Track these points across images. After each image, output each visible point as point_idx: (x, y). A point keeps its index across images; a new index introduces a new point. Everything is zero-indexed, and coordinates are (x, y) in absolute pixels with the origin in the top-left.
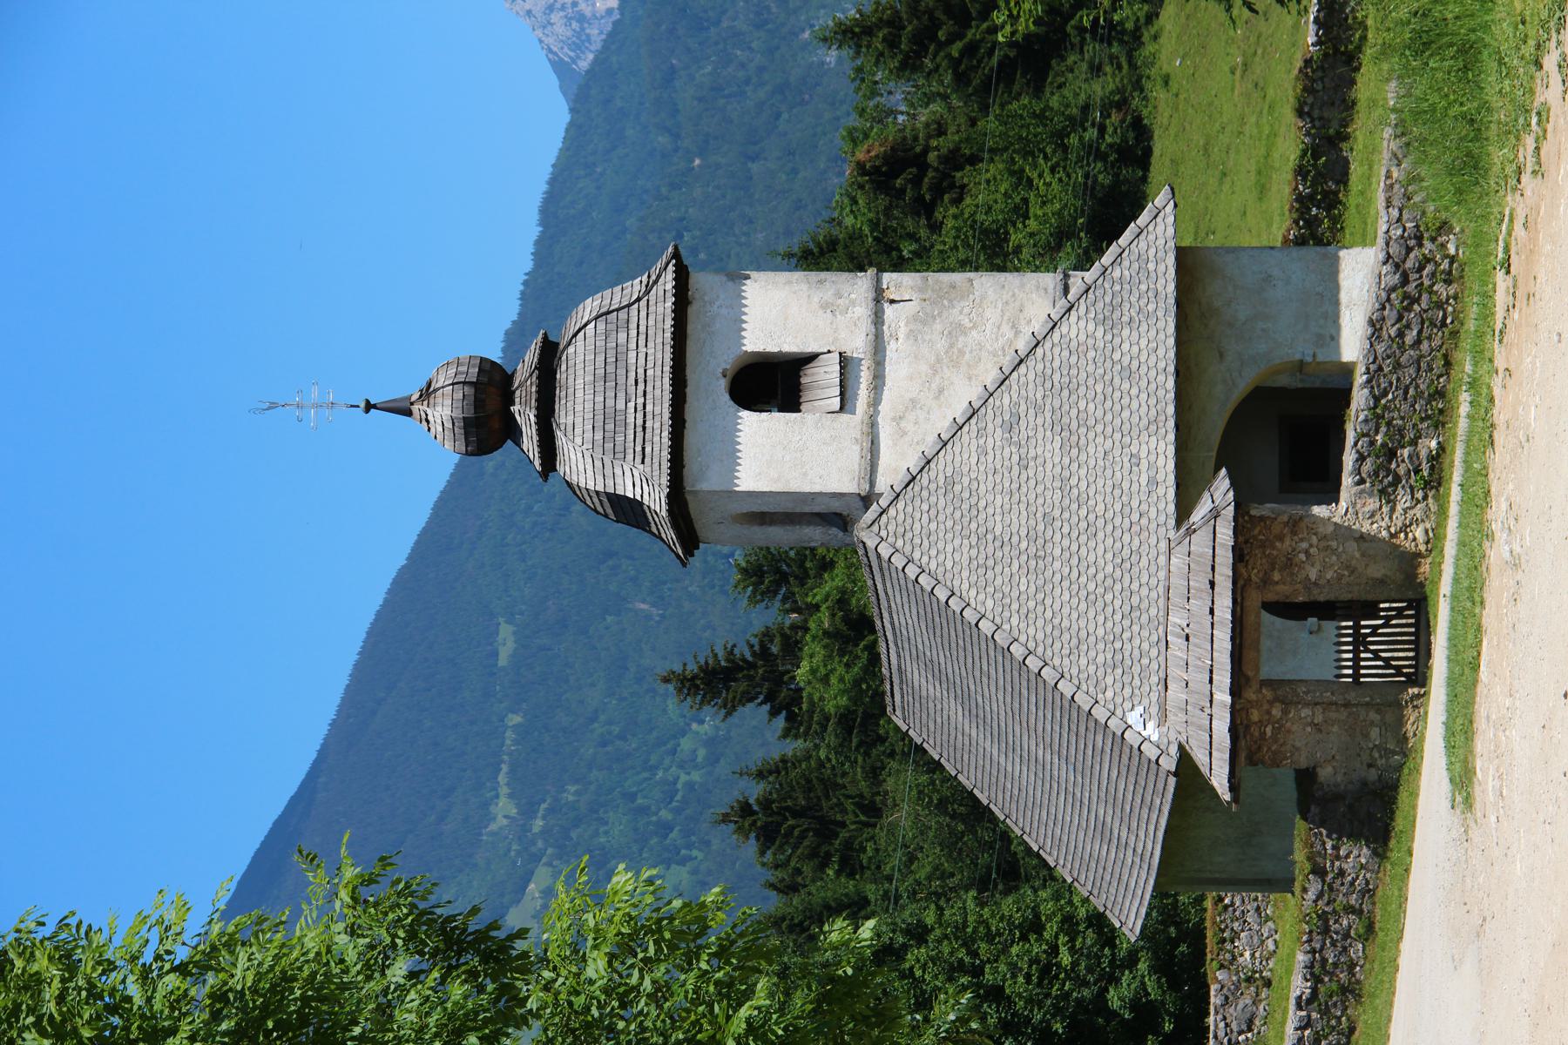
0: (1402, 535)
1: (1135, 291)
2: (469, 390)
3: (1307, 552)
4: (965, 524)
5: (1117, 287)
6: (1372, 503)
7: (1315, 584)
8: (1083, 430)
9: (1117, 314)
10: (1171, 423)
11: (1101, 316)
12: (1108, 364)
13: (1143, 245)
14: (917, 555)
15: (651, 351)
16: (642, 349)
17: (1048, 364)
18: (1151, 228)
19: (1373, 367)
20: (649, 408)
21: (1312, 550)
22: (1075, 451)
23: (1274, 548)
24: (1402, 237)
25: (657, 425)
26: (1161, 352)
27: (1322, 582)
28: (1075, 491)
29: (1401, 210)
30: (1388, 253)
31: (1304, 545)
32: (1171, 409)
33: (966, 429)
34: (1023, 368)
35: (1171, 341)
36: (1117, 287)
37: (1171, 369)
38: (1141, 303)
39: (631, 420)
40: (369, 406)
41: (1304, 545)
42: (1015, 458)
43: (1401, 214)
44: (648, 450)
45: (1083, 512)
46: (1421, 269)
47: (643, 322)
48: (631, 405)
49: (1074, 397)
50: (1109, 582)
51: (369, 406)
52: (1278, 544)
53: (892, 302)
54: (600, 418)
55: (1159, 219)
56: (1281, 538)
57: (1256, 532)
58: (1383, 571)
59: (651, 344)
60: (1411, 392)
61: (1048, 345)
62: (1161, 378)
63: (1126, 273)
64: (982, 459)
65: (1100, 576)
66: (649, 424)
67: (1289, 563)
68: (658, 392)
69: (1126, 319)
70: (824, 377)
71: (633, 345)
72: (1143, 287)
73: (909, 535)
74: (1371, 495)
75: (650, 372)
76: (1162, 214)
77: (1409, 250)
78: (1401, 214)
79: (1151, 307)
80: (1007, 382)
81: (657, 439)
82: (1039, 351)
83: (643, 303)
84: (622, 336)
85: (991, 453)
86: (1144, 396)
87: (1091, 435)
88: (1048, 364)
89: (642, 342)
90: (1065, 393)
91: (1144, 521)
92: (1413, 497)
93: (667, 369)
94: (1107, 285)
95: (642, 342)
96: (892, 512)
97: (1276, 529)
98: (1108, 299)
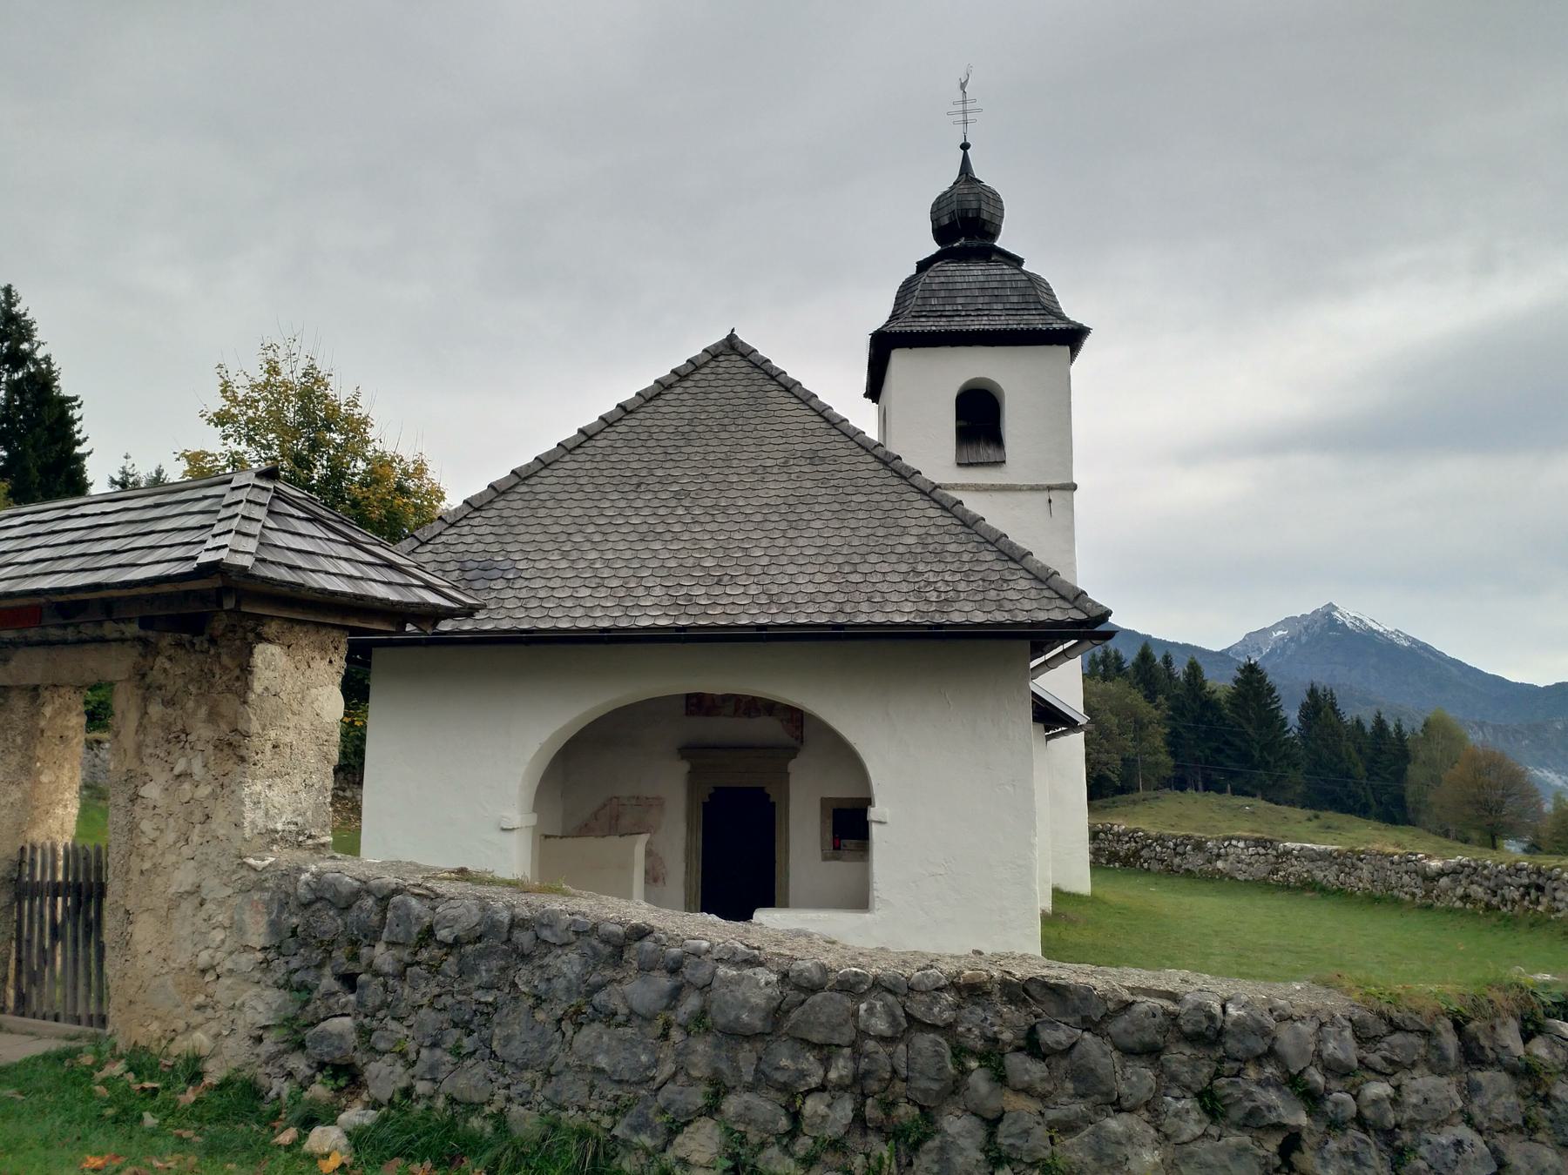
0: (200, 999)
1: (958, 577)
2: (974, 205)
3: (185, 775)
4: (705, 422)
5: (966, 557)
6: (258, 935)
7: (135, 798)
8: (783, 525)
9: (930, 558)
10: (763, 620)
11: (930, 540)
12: (864, 550)
13: (1024, 584)
14: (688, 384)
15: (1003, 318)
16: (1004, 312)
17: (877, 489)
18: (1047, 593)
19: (524, 939)
20: (957, 319)
21: (187, 786)
22: (759, 518)
23: (198, 705)
24: (864, 1034)
25: (941, 323)
26: (865, 607)
27: (138, 809)
28: (708, 518)
29: (947, 1029)
30: (814, 989)
31: (197, 768)
32: (781, 620)
33: (818, 419)
34: (876, 465)
35: (879, 618)
36: (966, 557)
37: (841, 619)
38: (939, 584)
39: (947, 308)
40: (965, 147)
41: (197, 768)
42: (769, 463)
43: (934, 1028)
44: (923, 319)
45: (677, 528)
46: (762, 1081)
47: (1026, 312)
48: (960, 308)
49: (828, 515)
50: (574, 555)
51: (965, 147)
52: (203, 712)
53: (1050, 501)
54: (950, 287)
55: (1059, 603)
56: (213, 717)
57: (226, 660)
58: (142, 949)
59: (1007, 318)
60: (468, 1044)
61: (904, 488)
62: (829, 607)
63: (985, 566)
64: (777, 434)
65: (587, 546)
66: (944, 319)
67: (178, 737)
68: (968, 323)
69: (921, 567)
70: (988, 453)
71: (1008, 306)
72: (962, 586)
73: (712, 377)
74: (274, 926)
75: (986, 318)
76: (1067, 605)
77: (826, 1052)
78: (934, 1028)
79: (933, 596)
80: (864, 452)
81: (930, 323)
82: (896, 481)
83: (1043, 312)
84: (1015, 299)
85: (784, 440)
86: (811, 589)
87: (777, 534)
88: (877, 489)
89: (1010, 312)
90: (836, 507)
91: (640, 592)
92: (265, 1028)
93: (987, 327)
94: (970, 546)
95: (1010, 312)
96: (744, 364)
97: (228, 705)
98: (952, 548)
